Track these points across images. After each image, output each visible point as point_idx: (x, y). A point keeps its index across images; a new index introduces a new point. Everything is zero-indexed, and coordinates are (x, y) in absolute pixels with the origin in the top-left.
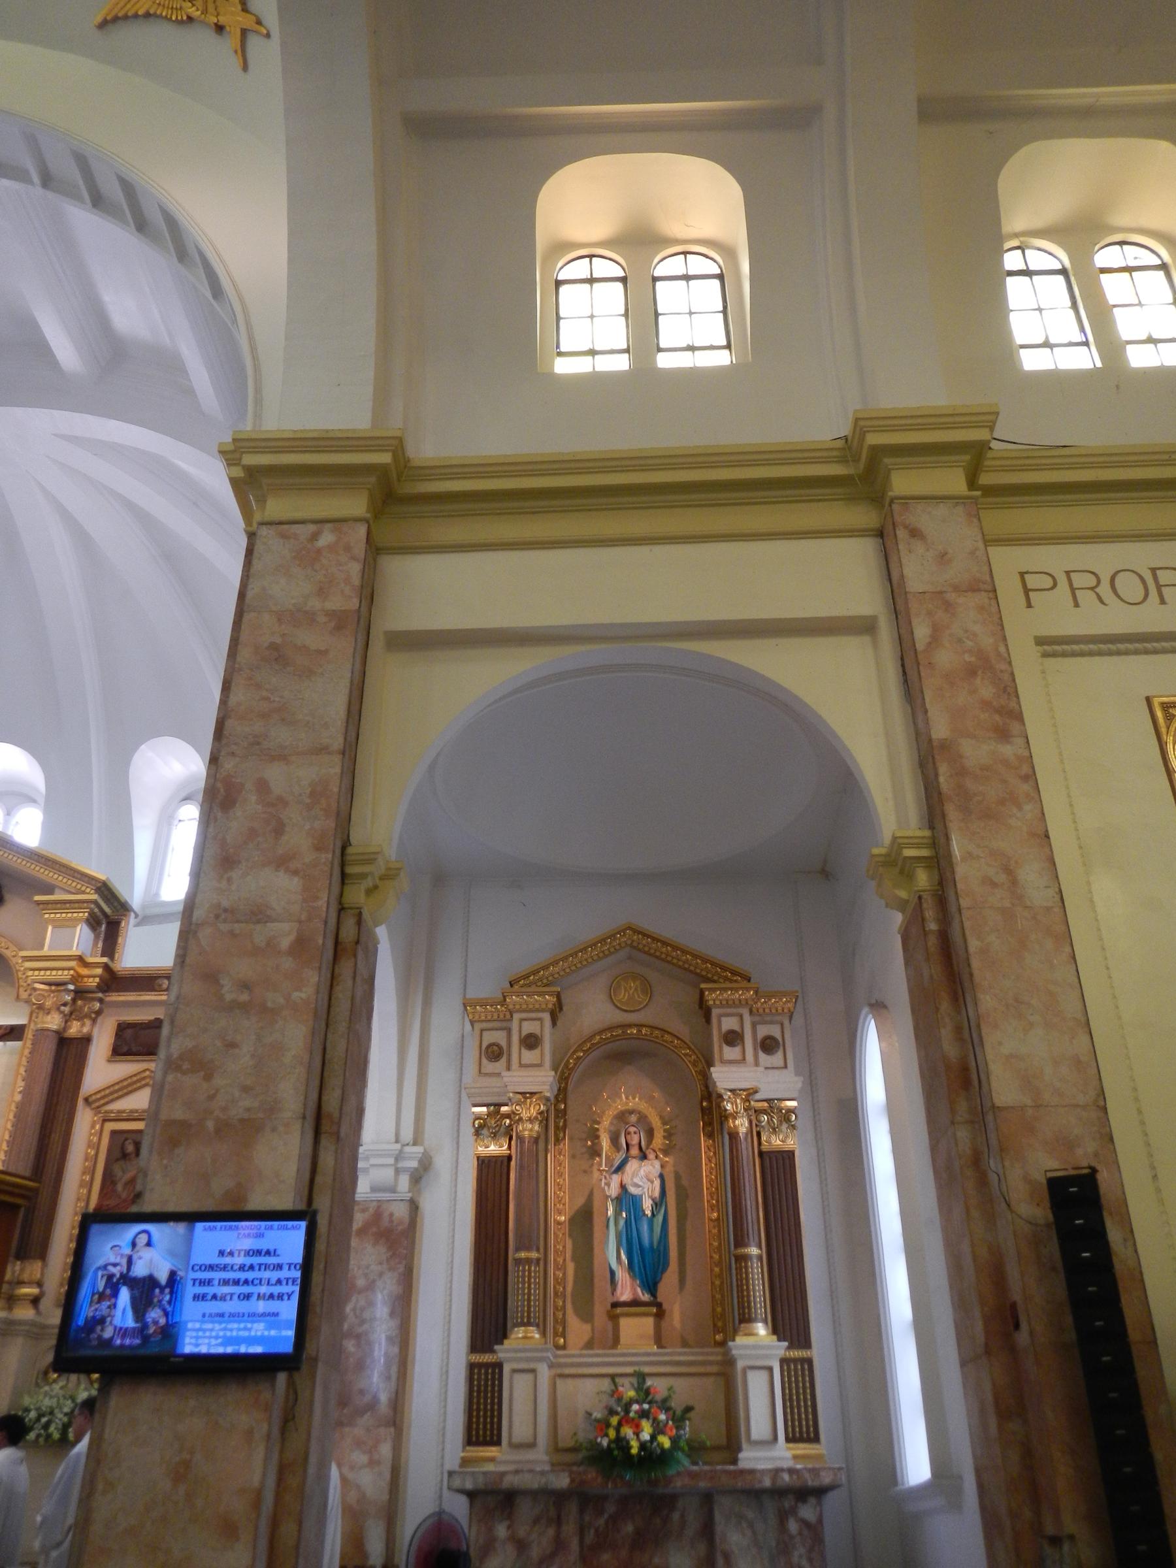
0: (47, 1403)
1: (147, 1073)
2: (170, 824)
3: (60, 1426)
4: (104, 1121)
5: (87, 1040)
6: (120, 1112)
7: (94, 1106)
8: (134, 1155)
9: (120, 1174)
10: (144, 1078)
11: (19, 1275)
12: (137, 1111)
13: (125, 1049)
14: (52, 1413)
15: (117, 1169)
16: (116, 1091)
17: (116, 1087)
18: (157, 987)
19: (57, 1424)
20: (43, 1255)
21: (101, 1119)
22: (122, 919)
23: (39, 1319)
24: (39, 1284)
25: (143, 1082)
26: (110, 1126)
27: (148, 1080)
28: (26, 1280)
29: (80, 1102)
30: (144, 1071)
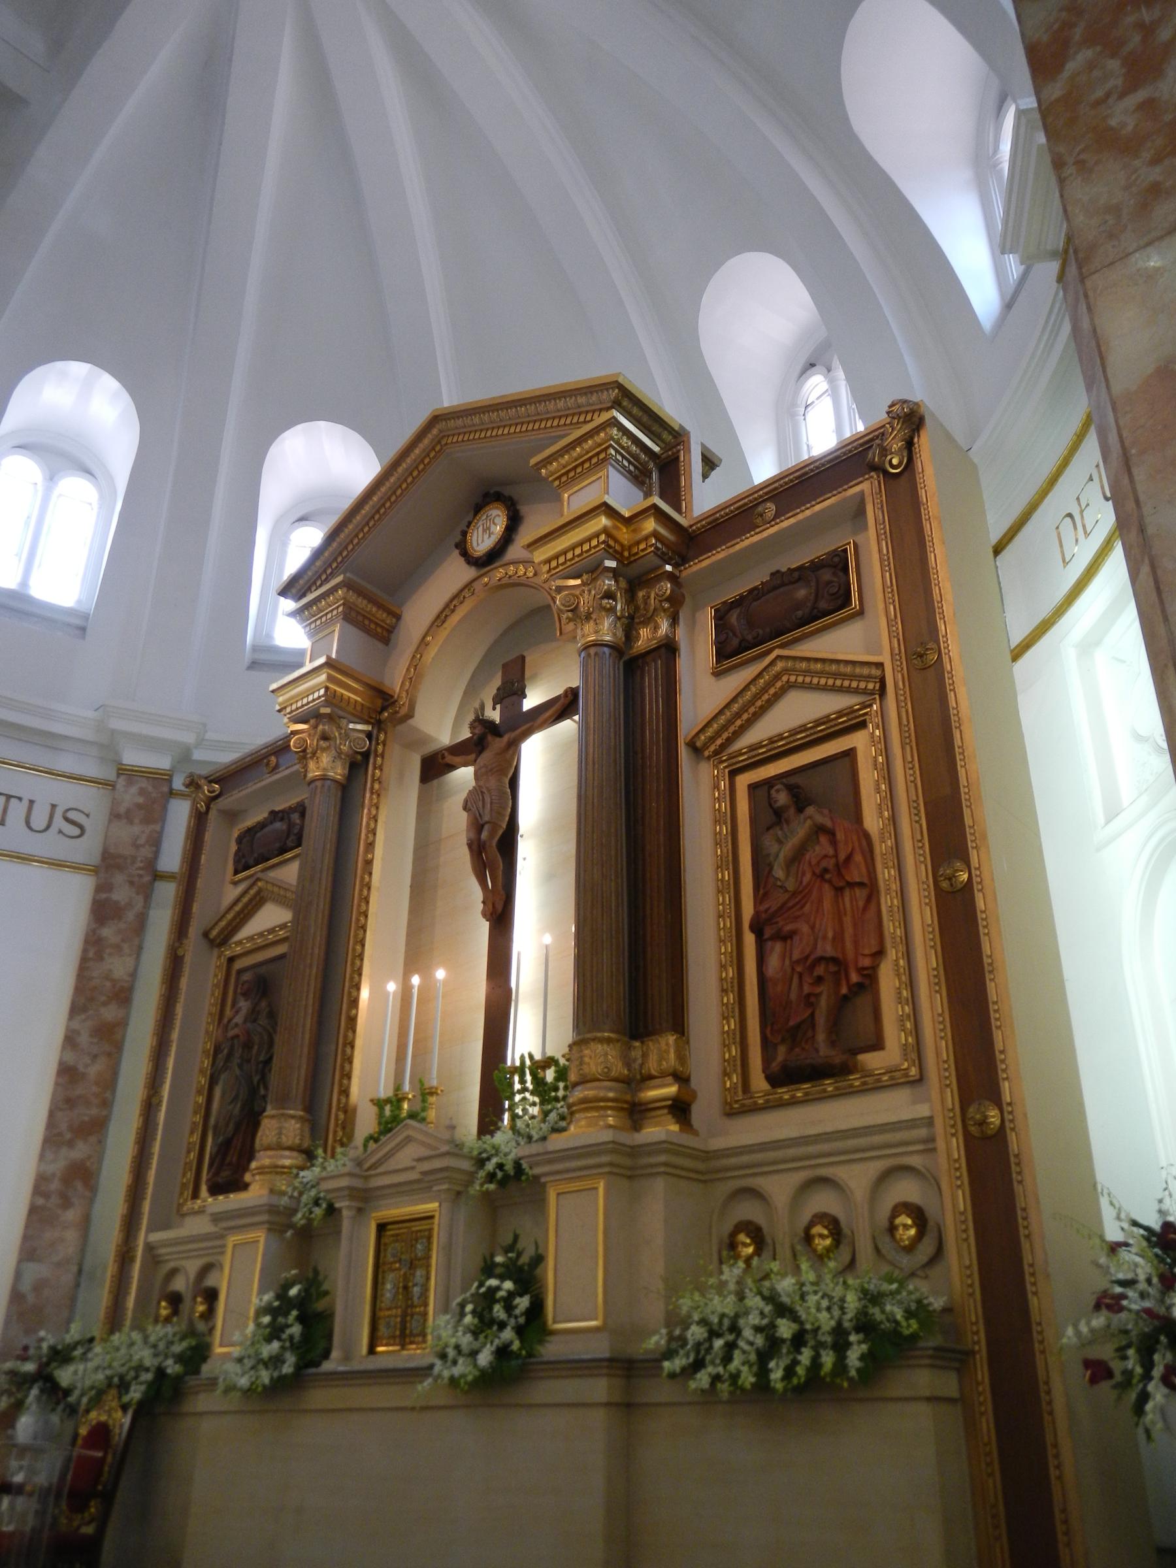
0: (721, 1305)
1: (780, 665)
2: (793, 416)
3: (753, 1357)
4: (733, 774)
5: (669, 649)
6: (753, 748)
7: (706, 753)
8: (792, 811)
9: (774, 848)
10: (777, 677)
11: (641, 1065)
12: (780, 737)
13: (735, 642)
14: (735, 1329)
15: (769, 843)
16: (738, 715)
17: (735, 707)
18: (759, 520)
19: (744, 1352)
20: (679, 1026)
21: (727, 770)
22: (679, 451)
23: (687, 1140)
24: (682, 1079)
25: (779, 684)
26: (744, 780)
27: (785, 678)
28: (654, 1072)
29: (684, 753)
30: (772, 663)
